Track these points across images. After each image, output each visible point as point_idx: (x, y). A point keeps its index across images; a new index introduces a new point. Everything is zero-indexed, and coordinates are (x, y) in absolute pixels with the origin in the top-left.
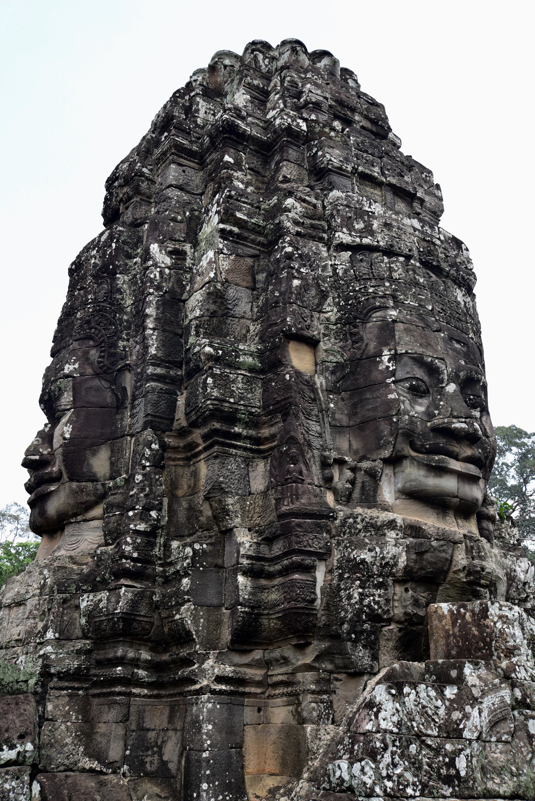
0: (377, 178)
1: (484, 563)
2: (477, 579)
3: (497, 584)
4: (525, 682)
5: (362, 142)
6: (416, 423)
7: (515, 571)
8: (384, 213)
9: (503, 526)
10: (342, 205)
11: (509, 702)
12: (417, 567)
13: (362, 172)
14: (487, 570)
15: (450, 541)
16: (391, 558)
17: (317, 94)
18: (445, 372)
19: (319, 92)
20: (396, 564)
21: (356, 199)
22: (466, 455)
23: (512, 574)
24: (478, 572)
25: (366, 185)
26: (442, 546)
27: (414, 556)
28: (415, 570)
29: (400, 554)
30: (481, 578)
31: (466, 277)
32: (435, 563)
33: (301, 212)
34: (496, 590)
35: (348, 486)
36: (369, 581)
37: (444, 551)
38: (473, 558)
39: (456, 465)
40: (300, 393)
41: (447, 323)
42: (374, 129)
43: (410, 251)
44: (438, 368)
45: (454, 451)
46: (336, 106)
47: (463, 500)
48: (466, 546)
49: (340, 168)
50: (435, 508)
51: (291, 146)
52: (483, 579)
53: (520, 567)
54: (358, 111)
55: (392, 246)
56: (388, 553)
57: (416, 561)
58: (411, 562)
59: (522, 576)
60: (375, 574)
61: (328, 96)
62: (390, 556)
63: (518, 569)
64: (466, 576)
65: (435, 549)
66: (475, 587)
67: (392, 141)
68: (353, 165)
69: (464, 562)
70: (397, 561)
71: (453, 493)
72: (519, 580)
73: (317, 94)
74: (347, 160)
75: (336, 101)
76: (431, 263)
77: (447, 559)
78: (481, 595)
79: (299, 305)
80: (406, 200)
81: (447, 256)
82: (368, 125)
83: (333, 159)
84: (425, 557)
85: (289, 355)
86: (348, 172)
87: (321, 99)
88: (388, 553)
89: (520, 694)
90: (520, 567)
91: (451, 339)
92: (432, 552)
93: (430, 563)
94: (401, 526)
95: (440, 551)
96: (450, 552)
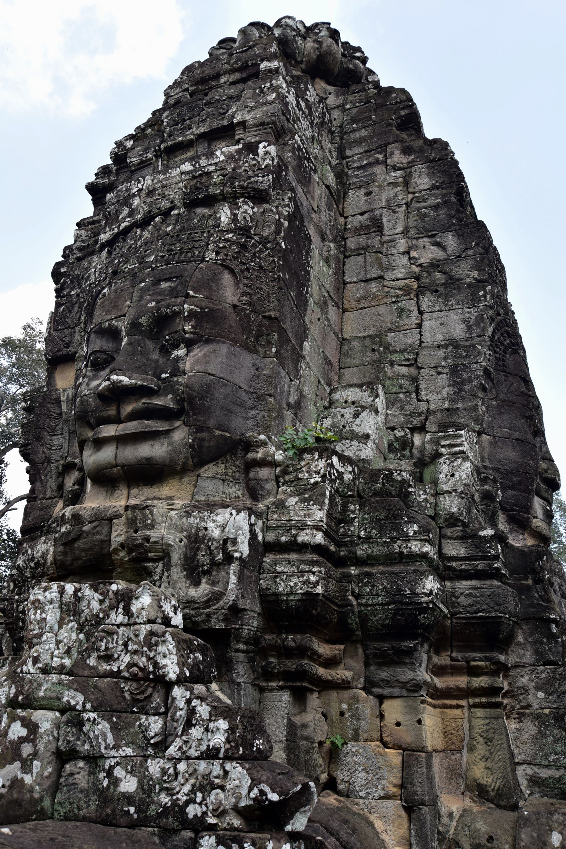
0: (182, 141)
1: (148, 533)
2: (141, 553)
3: (171, 553)
4: (28, 676)
5: (179, 115)
6: (87, 401)
7: (206, 529)
8: (153, 181)
9: (303, 463)
10: (113, 204)
11: (3, 702)
12: (69, 558)
13: (165, 148)
14: (151, 540)
15: (102, 519)
16: (40, 557)
17: (177, 94)
18: (123, 328)
19: (178, 90)
20: (45, 563)
21: (124, 189)
22: (126, 413)
23: (200, 534)
24: (141, 545)
25: (176, 157)
26: (95, 527)
27: (60, 549)
28: (69, 563)
29: (48, 550)
30: (146, 552)
31: (245, 184)
32: (91, 549)
33: (86, 236)
34: (170, 561)
35: (76, 487)
36: (24, 586)
37: (98, 533)
38: (136, 531)
39: (109, 431)
40: (45, 414)
41: (167, 265)
42: (244, 75)
43: (172, 202)
44: (117, 328)
45: (109, 415)
46: (197, 89)
47: (125, 466)
48: (127, 519)
49: (142, 162)
50: (104, 486)
51: (121, 171)
52: (151, 552)
53: (214, 521)
54: (222, 72)
55: (150, 212)
56: (37, 552)
57: (65, 553)
58: (59, 556)
59: (216, 533)
60: (29, 578)
61: (187, 86)
62: (39, 554)
63: (210, 525)
64: (129, 553)
65: (88, 533)
66: (143, 564)
67: (265, 71)
68: (153, 149)
69: (121, 539)
70: (46, 558)
71: (110, 464)
72: (212, 539)
73: (177, 94)
74: (146, 150)
75: (197, 83)
76: (198, 198)
77: (102, 541)
78: (152, 572)
79: (60, 330)
80: (227, 136)
81: (224, 176)
82: (237, 76)
83: (132, 160)
84: (76, 545)
85: (54, 380)
86: (150, 159)
87: (180, 94)
88: (37, 552)
89: (15, 690)
90: (214, 521)
91: (157, 282)
92: (85, 538)
93: (84, 550)
94: (68, 518)
95: (94, 534)
96: (105, 531)
